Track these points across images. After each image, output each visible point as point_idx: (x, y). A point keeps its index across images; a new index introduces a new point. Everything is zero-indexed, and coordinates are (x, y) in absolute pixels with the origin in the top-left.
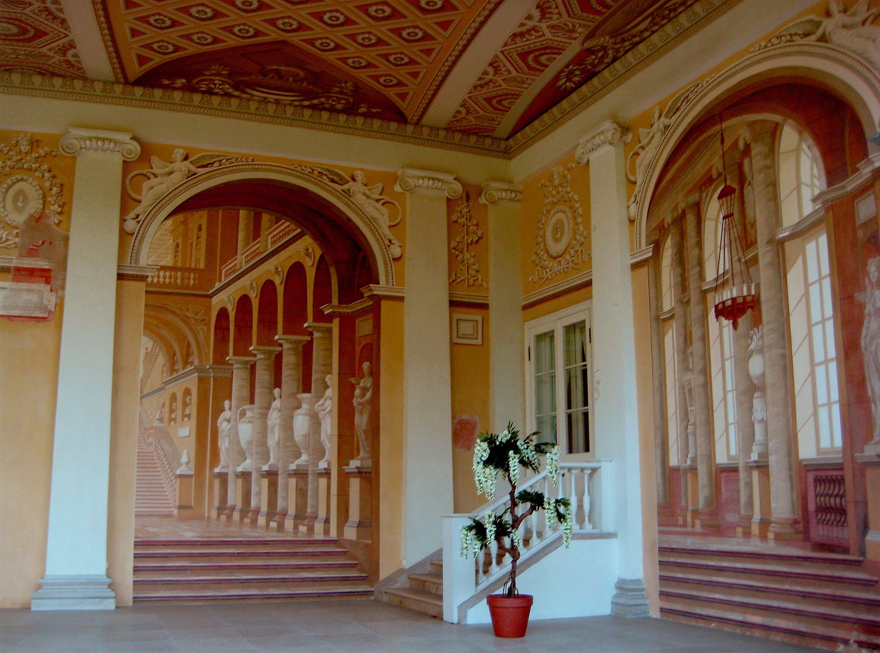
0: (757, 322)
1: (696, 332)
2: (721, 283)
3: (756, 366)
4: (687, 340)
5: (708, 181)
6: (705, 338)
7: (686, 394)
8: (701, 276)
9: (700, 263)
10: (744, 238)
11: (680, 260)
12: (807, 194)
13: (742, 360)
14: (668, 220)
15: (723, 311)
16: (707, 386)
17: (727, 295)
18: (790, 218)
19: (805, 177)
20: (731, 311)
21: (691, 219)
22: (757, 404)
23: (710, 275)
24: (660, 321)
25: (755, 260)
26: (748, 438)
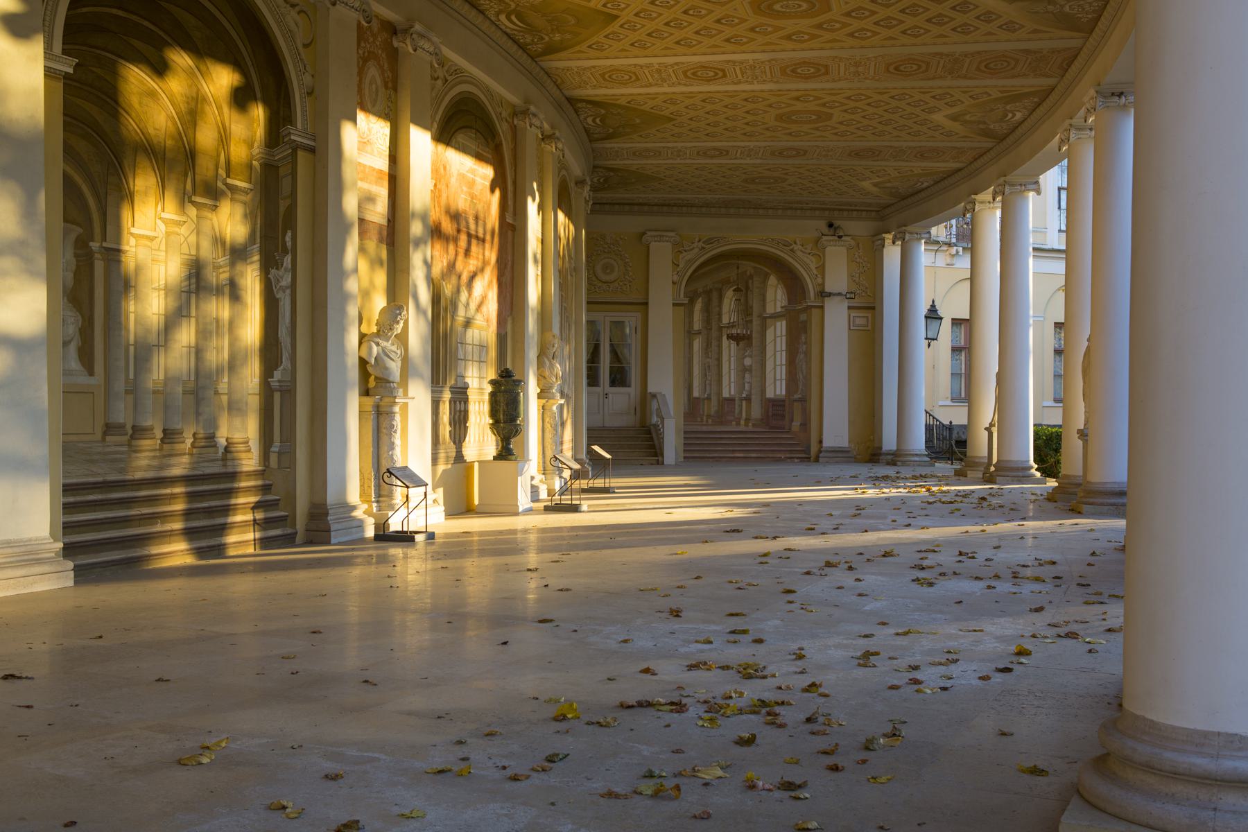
0: (750, 345)
1: (714, 343)
2: (731, 325)
3: (748, 362)
4: (707, 346)
5: (727, 282)
6: (720, 346)
7: (706, 370)
8: (720, 319)
9: (720, 314)
10: (746, 311)
11: (707, 309)
12: (779, 305)
13: (740, 359)
14: (701, 290)
15: (730, 337)
16: (719, 366)
17: (734, 331)
18: (770, 309)
19: (779, 297)
20: (736, 338)
21: (715, 295)
22: (747, 375)
23: (725, 320)
24: (690, 334)
25: (751, 321)
26: (741, 387)
